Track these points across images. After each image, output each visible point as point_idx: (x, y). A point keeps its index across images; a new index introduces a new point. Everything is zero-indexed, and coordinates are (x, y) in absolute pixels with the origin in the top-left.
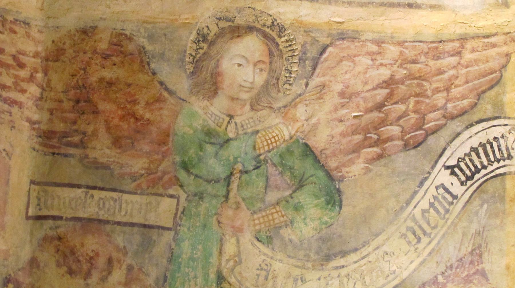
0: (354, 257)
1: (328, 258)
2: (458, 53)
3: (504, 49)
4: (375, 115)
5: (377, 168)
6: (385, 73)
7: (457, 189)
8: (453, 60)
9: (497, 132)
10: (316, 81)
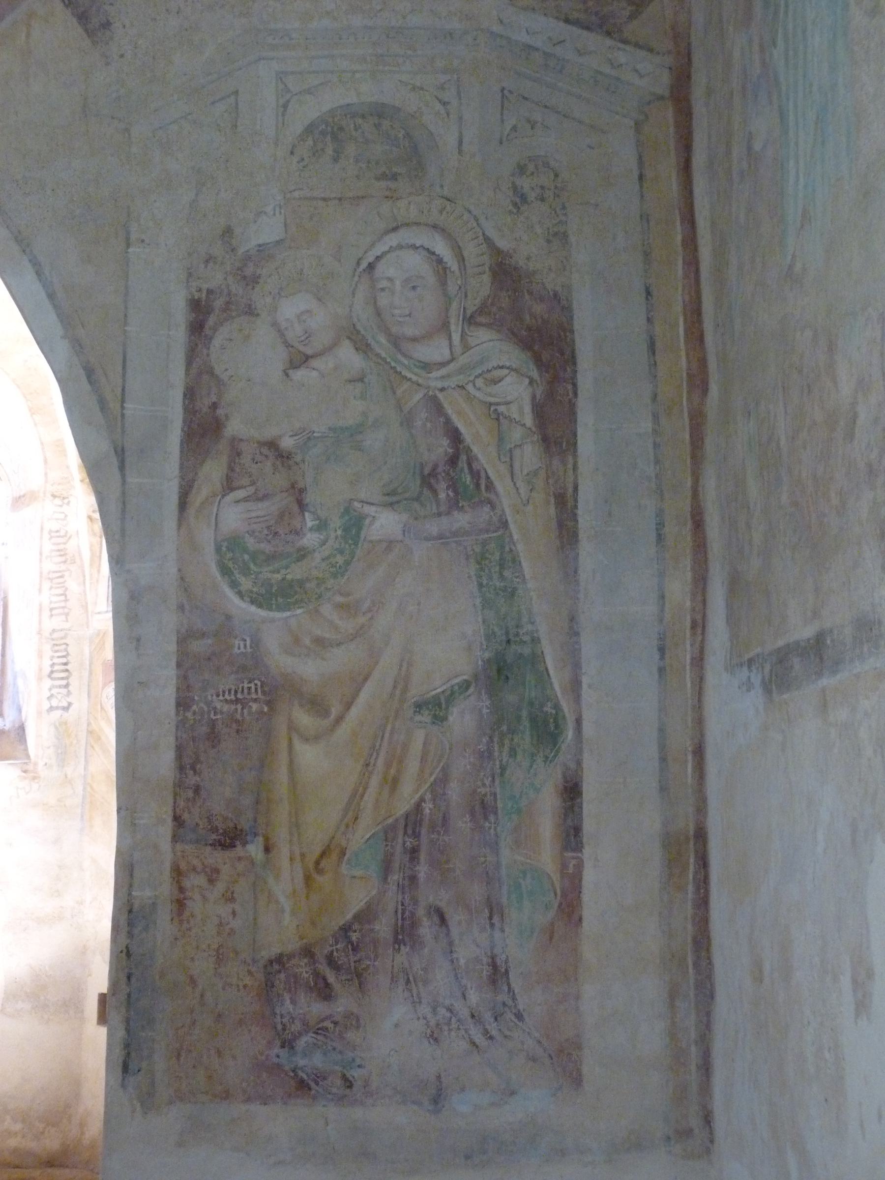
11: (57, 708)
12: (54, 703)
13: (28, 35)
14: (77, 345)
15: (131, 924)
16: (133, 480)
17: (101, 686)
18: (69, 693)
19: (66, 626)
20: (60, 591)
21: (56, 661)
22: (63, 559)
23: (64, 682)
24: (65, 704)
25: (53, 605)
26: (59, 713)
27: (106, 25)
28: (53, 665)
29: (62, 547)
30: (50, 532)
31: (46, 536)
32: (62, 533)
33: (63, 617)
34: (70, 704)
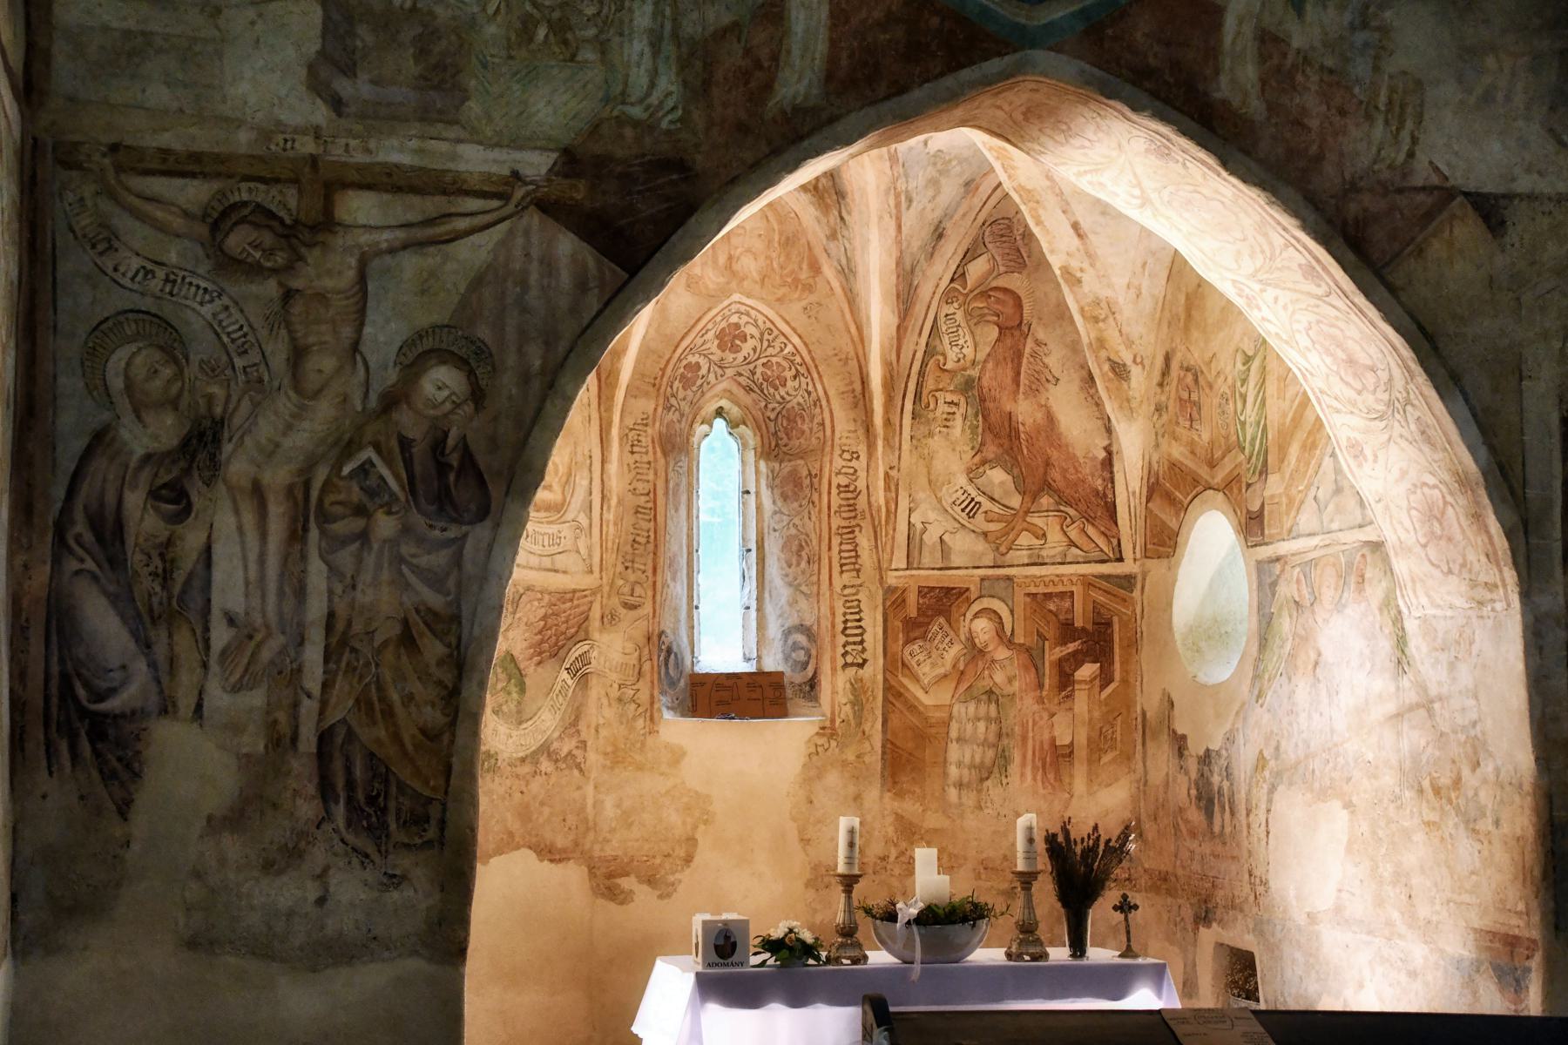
0: (530, 723)
1: (520, 723)
2: (571, 600)
3: (589, 599)
4: (539, 637)
5: (540, 669)
6: (542, 612)
7: (570, 682)
8: (568, 605)
9: (586, 648)
10: (518, 616)
11: (852, 665)
12: (849, 659)
13: (1451, 231)
14: (1492, 449)
15: (1553, 833)
16: (1534, 541)
17: (901, 642)
18: (864, 650)
19: (858, 582)
20: (849, 547)
21: (848, 617)
22: (853, 514)
23: (859, 639)
24: (861, 661)
25: (843, 561)
26: (855, 669)
27: (1503, 223)
28: (846, 622)
29: (852, 502)
30: (839, 486)
31: (834, 491)
32: (852, 488)
33: (854, 574)
34: (865, 661)
